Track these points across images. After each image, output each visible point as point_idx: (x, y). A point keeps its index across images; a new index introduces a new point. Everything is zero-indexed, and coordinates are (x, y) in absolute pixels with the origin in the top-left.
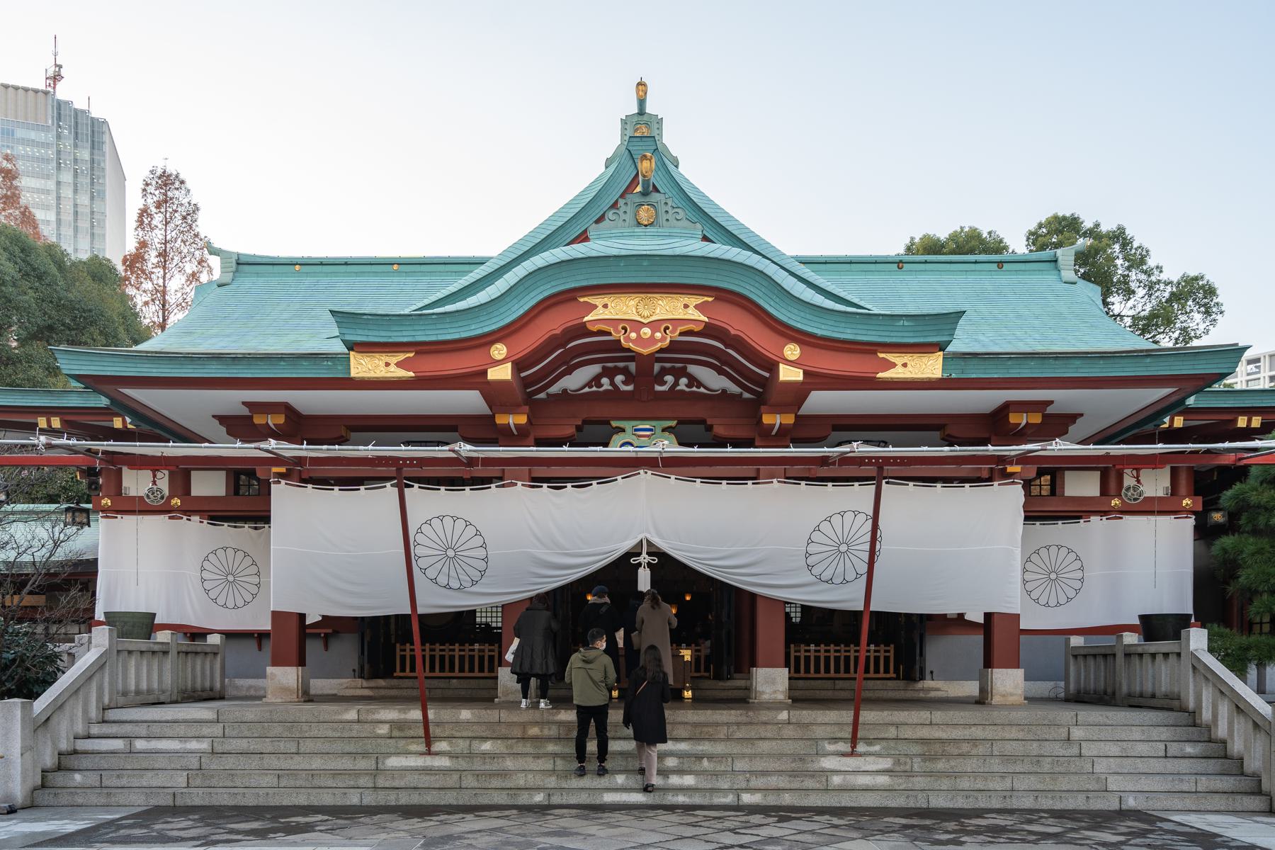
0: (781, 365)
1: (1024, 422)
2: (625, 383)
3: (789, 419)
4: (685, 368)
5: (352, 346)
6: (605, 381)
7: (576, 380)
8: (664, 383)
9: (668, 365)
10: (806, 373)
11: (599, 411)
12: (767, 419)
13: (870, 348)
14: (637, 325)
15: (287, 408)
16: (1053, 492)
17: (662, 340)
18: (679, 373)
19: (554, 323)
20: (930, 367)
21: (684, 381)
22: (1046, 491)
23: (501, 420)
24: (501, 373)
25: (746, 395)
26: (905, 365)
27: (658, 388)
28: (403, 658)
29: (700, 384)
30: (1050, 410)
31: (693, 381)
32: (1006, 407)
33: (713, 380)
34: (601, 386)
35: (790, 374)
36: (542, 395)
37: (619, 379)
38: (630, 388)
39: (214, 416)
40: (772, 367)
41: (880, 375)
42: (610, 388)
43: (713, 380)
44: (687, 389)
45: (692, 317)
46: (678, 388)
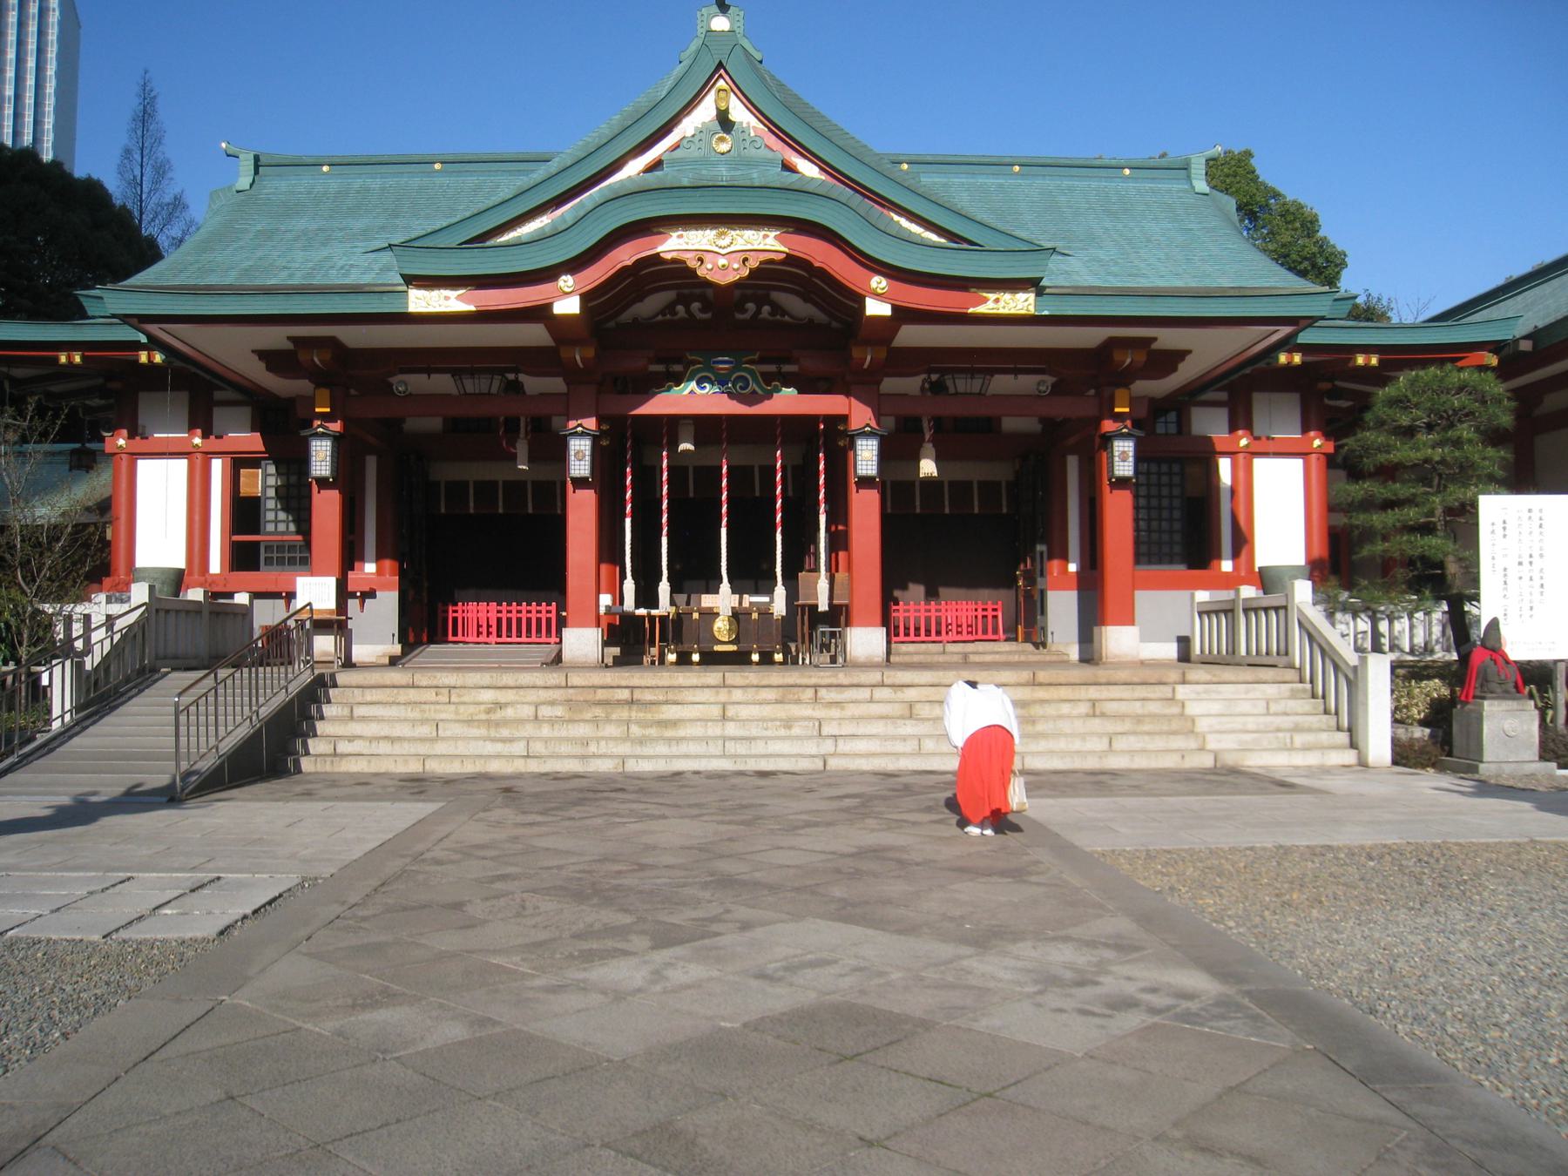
0: (867, 299)
1: (1129, 361)
2: (702, 310)
4: (768, 295)
6: (680, 308)
7: (649, 306)
8: (745, 311)
9: (749, 292)
10: (895, 308)
15: (333, 342)
16: (1180, 432)
18: (761, 301)
19: (626, 255)
20: (1021, 303)
21: (766, 309)
22: (1173, 429)
25: (835, 324)
26: (997, 301)
27: (739, 316)
28: (455, 620)
29: (784, 312)
30: (1155, 346)
31: (777, 308)
32: (1112, 343)
33: (797, 307)
34: (676, 314)
35: (876, 308)
36: (612, 324)
37: (696, 306)
38: (708, 316)
39: (253, 351)
41: (971, 310)
42: (686, 316)
43: (797, 307)
44: (771, 318)
45: (773, 248)
46: (761, 316)
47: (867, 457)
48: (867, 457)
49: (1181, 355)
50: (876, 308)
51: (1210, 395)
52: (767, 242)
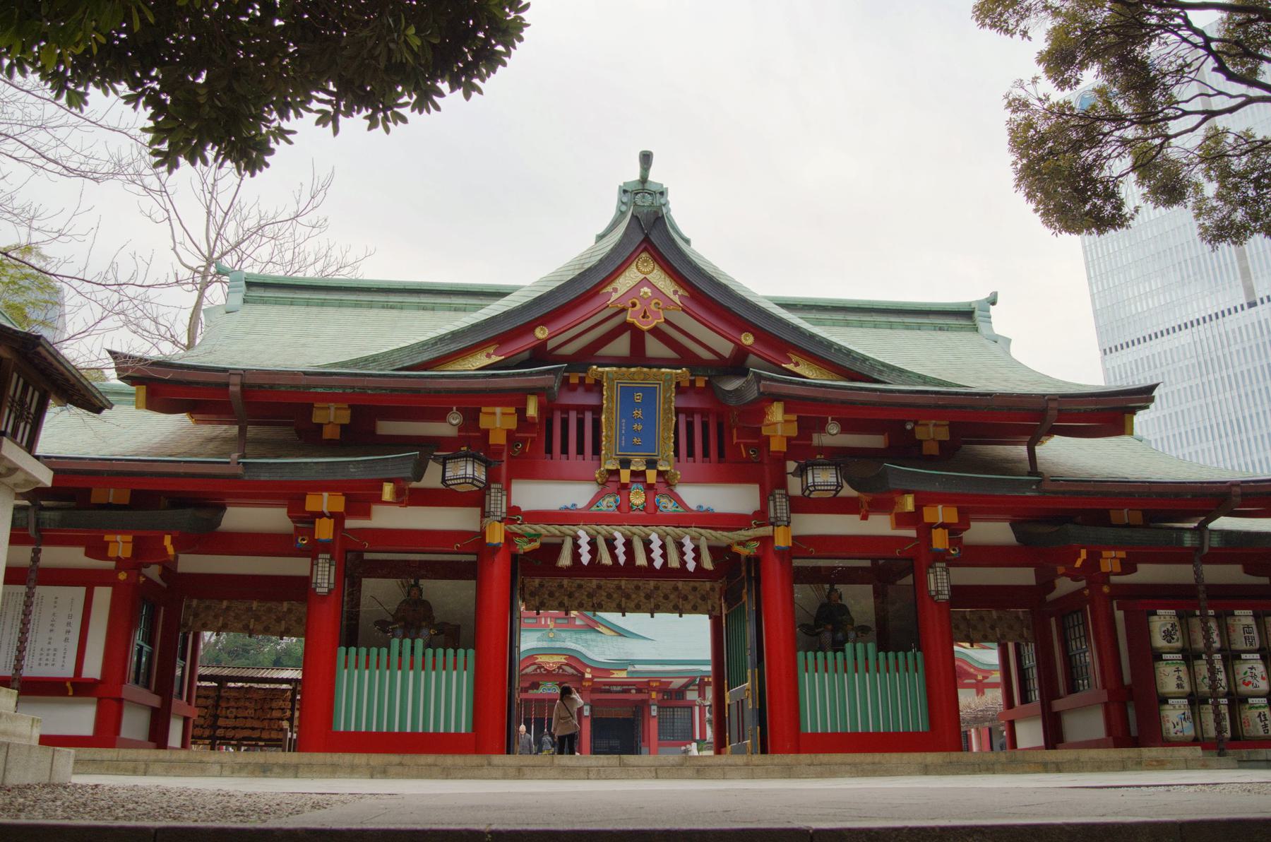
3: (590, 684)
11: (535, 680)
12: (584, 684)
13: (608, 670)
14: (549, 663)
20: (624, 674)
31: (563, 670)
32: (649, 682)
33: (569, 670)
40: (583, 674)
43: (568, 669)
49: (671, 682)
50: (588, 676)
51: (691, 687)
52: (562, 659)
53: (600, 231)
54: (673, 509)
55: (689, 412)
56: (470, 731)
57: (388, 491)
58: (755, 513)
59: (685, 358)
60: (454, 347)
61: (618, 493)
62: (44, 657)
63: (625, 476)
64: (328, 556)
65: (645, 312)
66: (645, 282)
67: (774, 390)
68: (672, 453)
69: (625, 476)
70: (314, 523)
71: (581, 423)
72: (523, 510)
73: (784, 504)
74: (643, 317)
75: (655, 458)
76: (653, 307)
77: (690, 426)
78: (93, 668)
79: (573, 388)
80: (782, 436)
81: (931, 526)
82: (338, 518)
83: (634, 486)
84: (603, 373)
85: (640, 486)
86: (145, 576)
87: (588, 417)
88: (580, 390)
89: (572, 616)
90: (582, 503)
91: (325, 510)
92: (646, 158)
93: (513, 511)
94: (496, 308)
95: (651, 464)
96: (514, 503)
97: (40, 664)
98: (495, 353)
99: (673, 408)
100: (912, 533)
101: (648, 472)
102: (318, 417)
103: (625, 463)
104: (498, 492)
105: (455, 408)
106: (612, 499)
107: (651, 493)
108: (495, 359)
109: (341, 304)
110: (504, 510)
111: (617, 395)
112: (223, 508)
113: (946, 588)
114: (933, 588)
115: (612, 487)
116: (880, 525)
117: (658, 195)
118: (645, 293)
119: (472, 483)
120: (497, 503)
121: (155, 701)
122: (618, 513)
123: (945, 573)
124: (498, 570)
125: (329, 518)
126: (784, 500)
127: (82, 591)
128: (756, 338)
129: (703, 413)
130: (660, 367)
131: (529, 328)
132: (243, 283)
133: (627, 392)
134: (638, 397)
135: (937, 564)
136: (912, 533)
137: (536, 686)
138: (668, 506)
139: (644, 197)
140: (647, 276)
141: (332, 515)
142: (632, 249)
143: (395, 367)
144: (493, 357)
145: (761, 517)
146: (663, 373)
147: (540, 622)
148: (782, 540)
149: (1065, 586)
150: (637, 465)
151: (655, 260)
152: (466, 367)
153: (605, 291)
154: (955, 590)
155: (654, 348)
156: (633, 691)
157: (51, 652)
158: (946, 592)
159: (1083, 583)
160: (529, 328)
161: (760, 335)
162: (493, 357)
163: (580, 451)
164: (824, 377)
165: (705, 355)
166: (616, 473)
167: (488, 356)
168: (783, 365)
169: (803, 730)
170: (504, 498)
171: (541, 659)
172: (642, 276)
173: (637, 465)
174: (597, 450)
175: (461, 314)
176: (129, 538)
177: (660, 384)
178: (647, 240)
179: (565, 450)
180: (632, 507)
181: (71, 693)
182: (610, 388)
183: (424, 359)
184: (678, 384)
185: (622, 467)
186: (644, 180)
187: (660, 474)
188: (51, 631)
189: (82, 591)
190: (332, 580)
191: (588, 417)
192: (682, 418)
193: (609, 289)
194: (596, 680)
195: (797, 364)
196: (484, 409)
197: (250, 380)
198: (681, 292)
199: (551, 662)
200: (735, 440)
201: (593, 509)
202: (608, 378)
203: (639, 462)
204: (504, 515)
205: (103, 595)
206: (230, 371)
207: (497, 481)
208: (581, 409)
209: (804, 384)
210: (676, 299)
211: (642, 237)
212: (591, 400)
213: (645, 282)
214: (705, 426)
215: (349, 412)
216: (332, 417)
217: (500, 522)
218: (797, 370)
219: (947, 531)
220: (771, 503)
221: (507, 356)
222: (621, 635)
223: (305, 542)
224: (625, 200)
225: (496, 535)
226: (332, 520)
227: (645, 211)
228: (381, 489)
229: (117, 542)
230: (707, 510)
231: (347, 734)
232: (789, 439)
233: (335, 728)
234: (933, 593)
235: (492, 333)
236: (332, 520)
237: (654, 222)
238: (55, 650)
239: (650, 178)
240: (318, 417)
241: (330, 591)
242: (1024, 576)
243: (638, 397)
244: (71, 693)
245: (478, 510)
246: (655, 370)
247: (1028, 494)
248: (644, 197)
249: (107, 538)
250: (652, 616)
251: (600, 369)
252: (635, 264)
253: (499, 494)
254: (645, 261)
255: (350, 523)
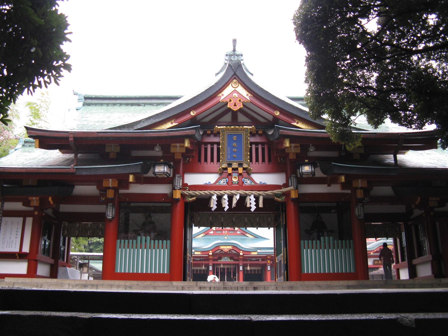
5: (195, 251)
7: (218, 252)
13: (250, 252)
14: (225, 249)
17: (228, 250)
23: (209, 257)
24: (211, 254)
31: (232, 252)
32: (267, 256)
33: (234, 252)
40: (239, 253)
47: (241, 268)
48: (241, 268)
50: (241, 254)
53: (217, 72)
54: (250, 183)
55: (257, 144)
56: (168, 272)
57: (131, 178)
58: (284, 184)
59: (254, 121)
60: (157, 120)
61: (228, 177)
62: (8, 244)
63: (230, 170)
64: (111, 204)
65: (235, 104)
66: (235, 91)
67: (284, 134)
68: (249, 161)
69: (230, 170)
70: (106, 191)
71: (212, 149)
72: (189, 185)
73: (295, 180)
74: (234, 106)
75: (242, 162)
76: (238, 101)
77: (257, 150)
78: (26, 249)
79: (209, 135)
80: (294, 153)
81: (356, 188)
82: (116, 190)
83: (234, 174)
84: (220, 128)
85: (236, 174)
86: (45, 213)
87: (215, 147)
88: (212, 136)
89: (236, 230)
90: (213, 182)
91: (110, 186)
92: (235, 41)
93: (185, 186)
94: (175, 104)
95: (240, 165)
96: (186, 182)
97: (7, 247)
98: (174, 122)
99: (249, 142)
100: (349, 191)
101: (239, 168)
102: (107, 150)
103: (230, 165)
104: (179, 178)
105: (158, 145)
106: (225, 180)
107: (241, 177)
108: (174, 124)
109: (121, 104)
110: (181, 185)
111: (226, 137)
112: (73, 186)
113: (362, 214)
114: (357, 214)
115: (225, 175)
116: (336, 189)
117: (240, 56)
118: (235, 96)
119: (166, 174)
120: (178, 183)
121: (52, 261)
122: (227, 185)
123: (362, 208)
124: (179, 209)
125: (112, 189)
126: (295, 179)
127: (21, 219)
128: (281, 113)
129: (262, 144)
130: (243, 126)
131: (187, 112)
132: (83, 98)
133: (230, 136)
134: (235, 138)
135: (359, 204)
136: (349, 191)
137: (220, 258)
138: (248, 182)
139: (234, 57)
140: (236, 89)
141: (113, 188)
142: (229, 78)
143: (134, 129)
144: (174, 123)
145: (286, 185)
146: (244, 128)
147: (223, 232)
148: (293, 195)
149: (417, 212)
150: (235, 165)
151: (239, 83)
152: (163, 128)
153: (218, 95)
154: (366, 215)
155: (241, 118)
156: (260, 260)
157: (11, 242)
158: (362, 216)
159: (423, 211)
160: (187, 112)
161: (282, 111)
162: (174, 123)
163: (212, 160)
164: (309, 128)
165: (262, 120)
166: (226, 169)
167: (172, 123)
168: (292, 124)
169: (303, 272)
170: (181, 180)
171: (222, 247)
172: (234, 89)
173: (235, 165)
174: (218, 160)
175: (155, 107)
176: (38, 198)
177: (243, 132)
178: (235, 74)
179: (206, 160)
180: (233, 183)
181: (18, 258)
182: (223, 135)
183: (146, 125)
184: (251, 133)
185: (229, 167)
186: (234, 50)
187: (244, 169)
188: (11, 234)
189: (21, 219)
190: (114, 214)
191: (215, 147)
192: (254, 146)
193: (220, 95)
194: (244, 256)
195: (298, 123)
196: (172, 145)
197: (76, 136)
198: (250, 95)
199: (226, 248)
200: (275, 155)
201: (217, 184)
202: (222, 131)
203: (235, 164)
204: (181, 187)
205: (30, 221)
206: (69, 133)
207: (178, 173)
208: (212, 144)
209: (300, 131)
210: (248, 98)
211: (233, 73)
212: (216, 140)
213: (235, 91)
214: (263, 149)
215: (120, 147)
216: (113, 149)
217: (179, 189)
218: (298, 125)
219: (362, 190)
220: (290, 180)
221: (179, 123)
222: (256, 237)
223: (104, 199)
224: (227, 58)
225: (177, 195)
226: (113, 190)
227: (234, 63)
228: (128, 177)
229: (33, 200)
230: (264, 184)
231: (121, 273)
232: (297, 154)
233: (116, 271)
234: (357, 216)
235: (172, 114)
236: (113, 190)
237: (238, 67)
238: (12, 241)
239: (237, 49)
240: (107, 150)
241: (113, 218)
242: (400, 209)
243: (235, 138)
244: (18, 258)
245: (171, 185)
246: (241, 127)
247: (393, 174)
248: (234, 57)
249: (30, 198)
250: (257, 229)
251: (219, 127)
252: (231, 84)
253: (179, 179)
254: (235, 83)
255: (121, 191)
